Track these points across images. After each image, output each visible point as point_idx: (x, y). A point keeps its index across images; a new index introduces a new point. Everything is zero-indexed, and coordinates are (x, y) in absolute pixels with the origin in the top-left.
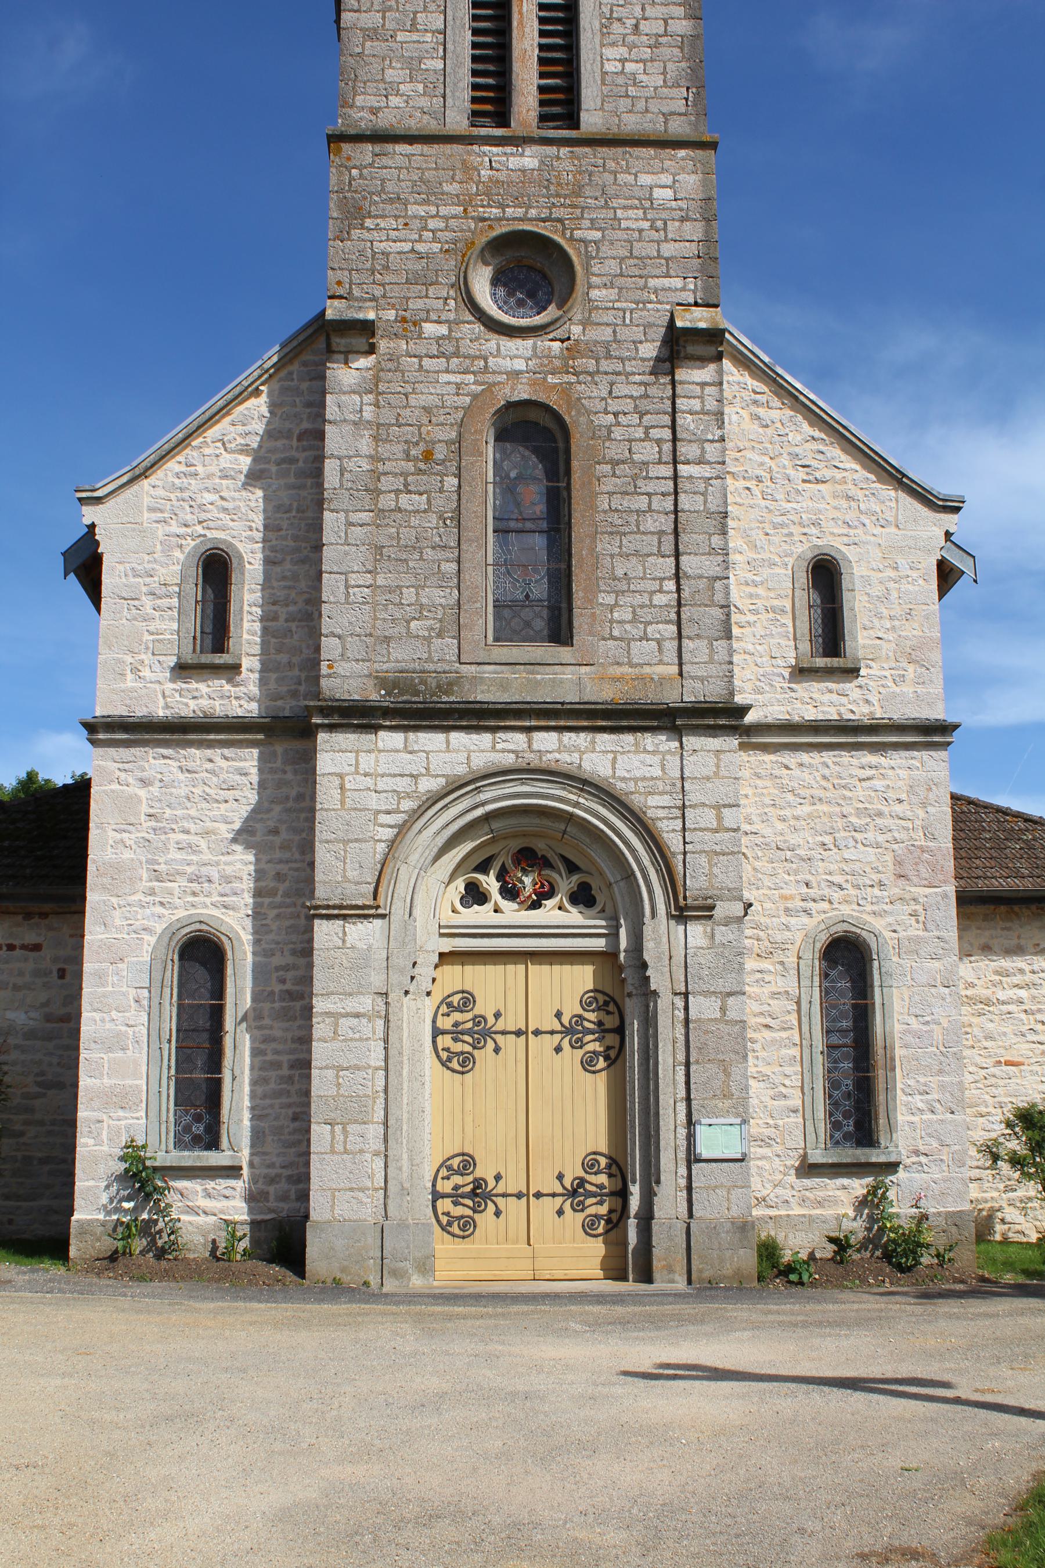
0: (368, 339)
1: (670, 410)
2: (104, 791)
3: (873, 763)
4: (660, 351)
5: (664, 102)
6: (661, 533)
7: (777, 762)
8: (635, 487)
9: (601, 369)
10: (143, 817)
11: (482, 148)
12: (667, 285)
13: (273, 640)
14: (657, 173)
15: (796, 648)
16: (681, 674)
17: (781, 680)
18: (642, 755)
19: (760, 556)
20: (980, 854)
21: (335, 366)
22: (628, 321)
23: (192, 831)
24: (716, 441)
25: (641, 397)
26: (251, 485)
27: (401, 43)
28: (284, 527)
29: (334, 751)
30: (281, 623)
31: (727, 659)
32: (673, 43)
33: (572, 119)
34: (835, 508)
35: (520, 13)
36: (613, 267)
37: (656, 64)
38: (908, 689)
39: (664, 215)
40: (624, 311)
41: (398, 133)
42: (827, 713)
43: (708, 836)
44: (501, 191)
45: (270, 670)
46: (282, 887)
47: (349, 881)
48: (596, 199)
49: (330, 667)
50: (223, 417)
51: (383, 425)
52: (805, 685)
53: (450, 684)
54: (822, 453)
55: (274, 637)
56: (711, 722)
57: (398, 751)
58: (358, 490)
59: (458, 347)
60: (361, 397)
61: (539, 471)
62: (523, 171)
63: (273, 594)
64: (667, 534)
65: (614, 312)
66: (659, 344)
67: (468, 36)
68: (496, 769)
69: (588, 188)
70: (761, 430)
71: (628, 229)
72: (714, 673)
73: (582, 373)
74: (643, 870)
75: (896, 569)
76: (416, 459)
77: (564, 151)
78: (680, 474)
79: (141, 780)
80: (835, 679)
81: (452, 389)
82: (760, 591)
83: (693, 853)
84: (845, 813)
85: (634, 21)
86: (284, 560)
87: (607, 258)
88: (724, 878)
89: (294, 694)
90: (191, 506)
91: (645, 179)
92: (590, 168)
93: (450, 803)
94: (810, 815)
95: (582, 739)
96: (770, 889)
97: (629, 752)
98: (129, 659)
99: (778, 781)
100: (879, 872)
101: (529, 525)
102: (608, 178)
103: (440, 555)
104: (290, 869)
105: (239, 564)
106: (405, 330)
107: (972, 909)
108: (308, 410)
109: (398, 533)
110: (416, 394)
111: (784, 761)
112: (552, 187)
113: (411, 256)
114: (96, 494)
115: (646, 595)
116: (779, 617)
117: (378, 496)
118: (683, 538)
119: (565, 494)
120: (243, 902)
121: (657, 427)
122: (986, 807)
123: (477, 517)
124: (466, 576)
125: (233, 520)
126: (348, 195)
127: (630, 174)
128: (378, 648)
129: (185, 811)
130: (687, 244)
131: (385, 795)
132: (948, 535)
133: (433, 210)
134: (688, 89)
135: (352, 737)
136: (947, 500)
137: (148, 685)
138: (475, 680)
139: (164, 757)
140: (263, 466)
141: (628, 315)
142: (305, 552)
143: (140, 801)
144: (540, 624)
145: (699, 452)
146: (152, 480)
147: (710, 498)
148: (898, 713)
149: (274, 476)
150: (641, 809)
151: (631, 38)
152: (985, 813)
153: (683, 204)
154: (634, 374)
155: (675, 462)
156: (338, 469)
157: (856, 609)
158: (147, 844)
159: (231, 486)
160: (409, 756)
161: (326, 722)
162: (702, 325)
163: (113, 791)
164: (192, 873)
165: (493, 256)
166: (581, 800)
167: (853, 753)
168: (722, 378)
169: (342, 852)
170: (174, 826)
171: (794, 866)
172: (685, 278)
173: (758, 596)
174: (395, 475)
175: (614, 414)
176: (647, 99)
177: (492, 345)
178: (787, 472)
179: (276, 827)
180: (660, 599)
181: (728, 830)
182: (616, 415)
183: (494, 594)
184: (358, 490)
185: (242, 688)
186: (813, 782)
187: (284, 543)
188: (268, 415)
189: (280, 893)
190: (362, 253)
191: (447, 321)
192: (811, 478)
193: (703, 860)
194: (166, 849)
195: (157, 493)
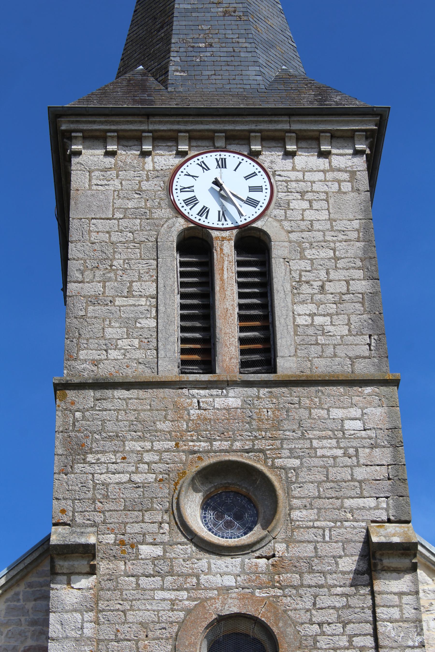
1: (371, 619)
4: (358, 565)
5: (350, 347)
11: (191, 391)
21: (58, 586)
22: (327, 538)
24: (417, 647)
25: (343, 607)
32: (355, 300)
35: (222, 280)
39: (355, 443)
40: (324, 529)
41: (117, 381)
44: (209, 427)
48: (294, 431)
51: (102, 640)
59: (172, 566)
60: (82, 615)
62: (228, 409)
65: (314, 530)
66: (357, 558)
67: (177, 299)
69: (286, 422)
71: (323, 456)
73: (287, 587)
77: (263, 391)
81: (166, 605)
85: (320, 283)
87: (305, 482)
91: (337, 413)
92: (287, 405)
102: (304, 413)
106: (123, 552)
108: (33, 629)
110: (133, 610)
112: (254, 423)
113: (128, 485)
121: (360, 635)
126: (73, 434)
127: (323, 409)
130: (378, 468)
134: (370, 336)
141: (327, 533)
153: (372, 433)
154: (335, 586)
162: (396, 540)
165: (202, 484)
168: (418, 588)
172: (377, 498)
175: (319, 624)
176: (335, 346)
177: (204, 561)
182: (320, 625)
190: (84, 485)
191: (162, 543)
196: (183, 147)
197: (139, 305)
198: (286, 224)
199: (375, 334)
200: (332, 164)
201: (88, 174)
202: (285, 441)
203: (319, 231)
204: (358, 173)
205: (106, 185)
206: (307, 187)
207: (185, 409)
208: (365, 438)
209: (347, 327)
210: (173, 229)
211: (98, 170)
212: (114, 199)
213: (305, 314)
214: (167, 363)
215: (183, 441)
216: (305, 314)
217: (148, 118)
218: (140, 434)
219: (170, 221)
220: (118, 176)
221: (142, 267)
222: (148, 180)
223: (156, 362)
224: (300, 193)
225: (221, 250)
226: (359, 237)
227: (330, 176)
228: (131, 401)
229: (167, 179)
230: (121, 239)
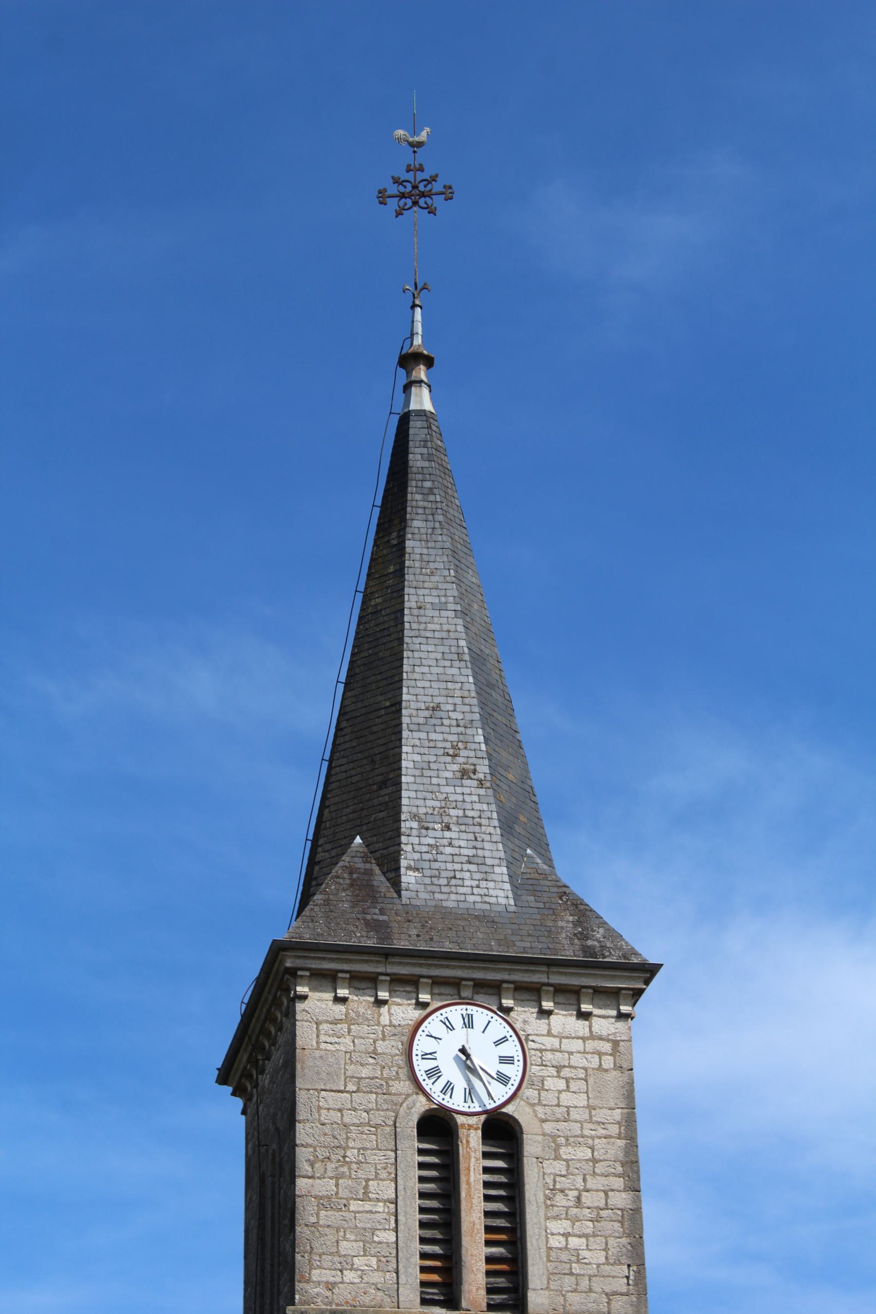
32: (614, 1217)
35: (468, 1183)
85: (576, 1193)
134: (629, 1266)
196: (424, 997)
197: (376, 1212)
198: (539, 1109)
199: (634, 1264)
200: (593, 1029)
201: (315, 1026)
204: (622, 1043)
205: (336, 1043)
206: (563, 1059)
209: (604, 1253)
210: (413, 1110)
211: (327, 1022)
212: (345, 1064)
213: (559, 1234)
214: (408, 1292)
216: (559, 1234)
217: (386, 958)
219: (410, 1099)
220: (349, 1031)
221: (378, 1158)
222: (383, 1039)
223: (396, 1288)
224: (556, 1067)
225: (468, 1142)
226: (620, 1132)
227: (591, 1045)
229: (405, 1039)
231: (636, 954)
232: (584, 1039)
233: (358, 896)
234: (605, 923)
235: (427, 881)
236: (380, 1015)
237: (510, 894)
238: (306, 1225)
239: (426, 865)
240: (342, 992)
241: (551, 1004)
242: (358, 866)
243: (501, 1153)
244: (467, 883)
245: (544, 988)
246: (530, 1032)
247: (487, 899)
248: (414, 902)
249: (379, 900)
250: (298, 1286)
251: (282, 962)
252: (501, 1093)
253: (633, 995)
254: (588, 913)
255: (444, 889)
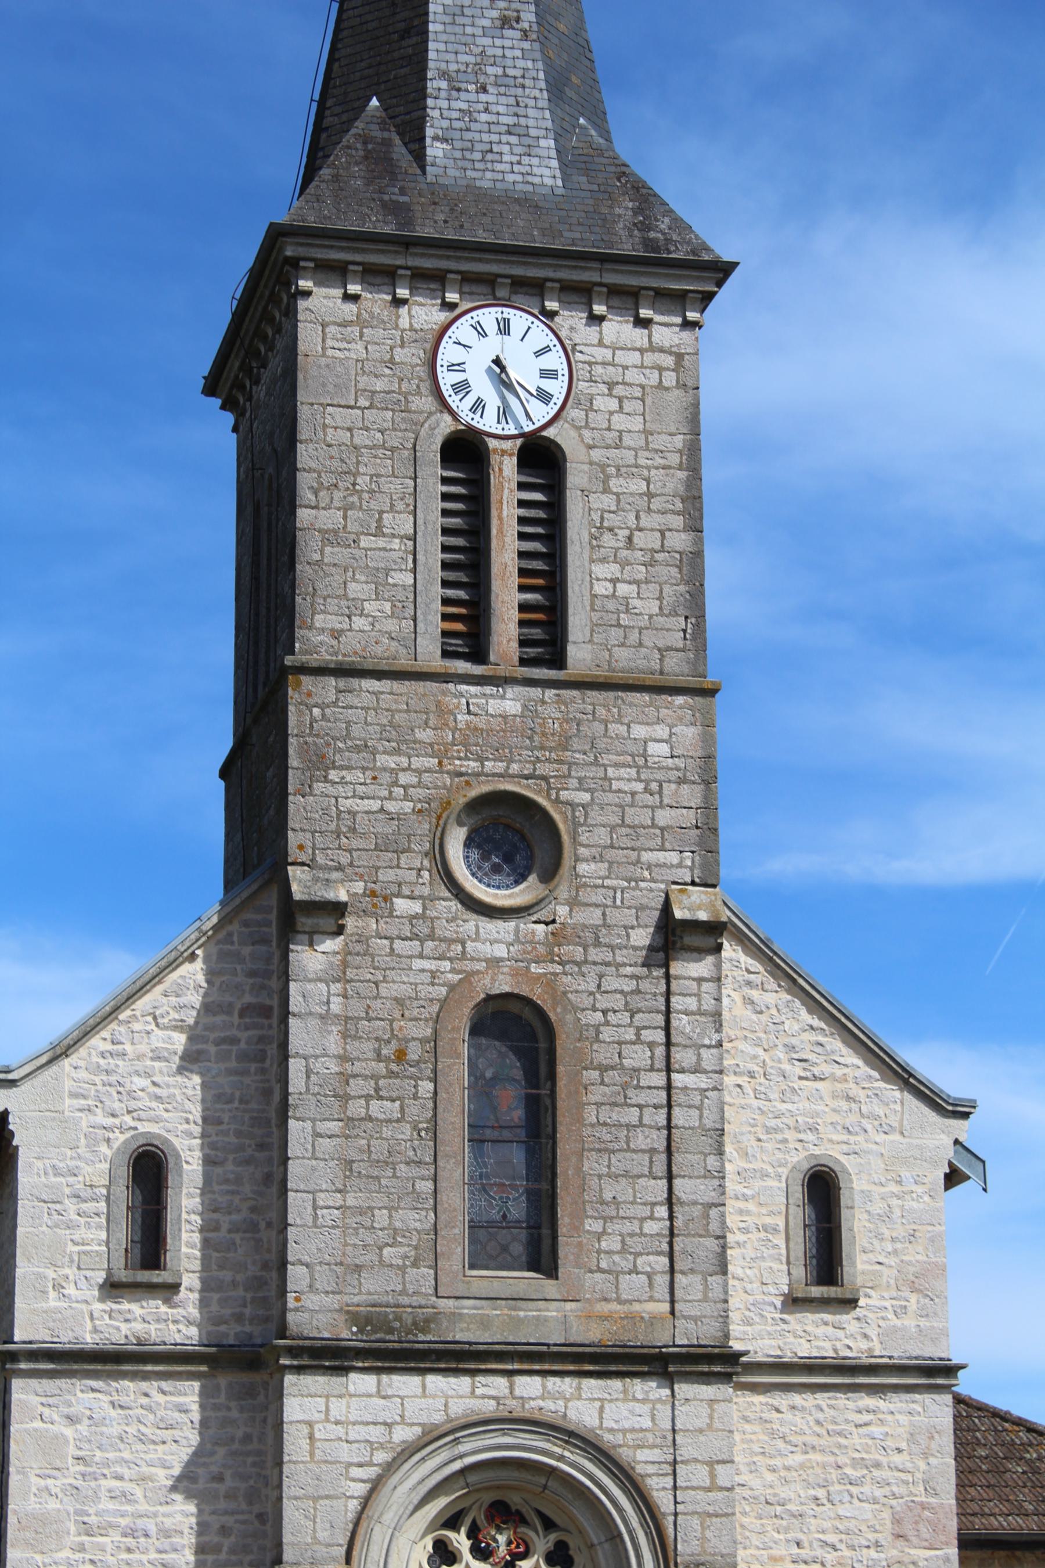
0: (337, 920)
1: (663, 1008)
2: (25, 1430)
3: (872, 1407)
4: (653, 939)
6: (652, 1151)
7: (767, 1404)
8: (625, 1097)
9: (590, 959)
10: (70, 1460)
11: (459, 687)
12: (662, 860)
13: (215, 1254)
14: (653, 724)
15: (789, 1274)
16: (672, 1312)
17: (772, 1309)
18: (631, 1404)
19: (751, 1166)
20: (975, 1480)
21: (299, 948)
22: (618, 902)
23: (126, 1477)
25: (632, 992)
26: (187, 1070)
27: (366, 550)
28: (226, 1120)
29: (302, 1396)
30: (223, 1233)
31: (722, 1297)
33: (557, 658)
34: (834, 1110)
35: (500, 518)
36: (602, 836)
37: (651, 586)
38: (909, 1322)
39: (659, 776)
41: (366, 667)
42: (823, 1348)
43: (700, 1495)
44: (480, 741)
45: (212, 1290)
46: (227, 1543)
47: (320, 1543)
48: (585, 754)
49: (297, 1299)
50: (154, 986)
51: (351, 1018)
52: (799, 1316)
53: (427, 1321)
54: (821, 1045)
55: (218, 1251)
56: (705, 1368)
57: (370, 1396)
58: (326, 1096)
59: (433, 928)
60: (328, 986)
61: (518, 1074)
62: (504, 717)
63: (214, 1200)
64: (659, 1152)
65: (604, 891)
66: (652, 930)
68: (475, 1418)
69: (575, 740)
70: (754, 1017)
71: (620, 791)
72: (709, 1312)
73: (569, 962)
74: (630, 1532)
75: (900, 1183)
76: (387, 1060)
77: (550, 693)
78: (674, 1084)
79: (68, 1417)
80: (831, 1309)
81: (426, 977)
82: (751, 1206)
83: (685, 1514)
84: (840, 1463)
85: (627, 532)
86: (226, 1160)
87: (596, 825)
88: (718, 1544)
89: (239, 1318)
90: (119, 1093)
91: (639, 731)
92: (579, 716)
93: (427, 1456)
94: (802, 1466)
95: (566, 1385)
96: (758, 1548)
97: (617, 1400)
98: (51, 1274)
99: (768, 1426)
100: (876, 1531)
101: (506, 1134)
102: (598, 727)
103: (415, 1171)
104: (236, 1521)
105: (176, 1164)
107: (969, 1553)
108: (251, 981)
109: (369, 1146)
110: (387, 982)
111: (776, 1403)
112: (536, 738)
113: (380, 816)
114: (10, 1076)
115: (636, 1223)
116: (770, 1237)
117: (347, 1102)
118: (677, 1158)
119: (548, 1102)
120: (183, 1560)
121: (650, 1027)
122: (979, 1409)
123: (455, 1129)
124: (442, 1197)
125: (167, 1110)
126: (310, 740)
127: (622, 724)
128: (348, 1278)
129: (118, 1454)
130: (684, 811)
131: (356, 1445)
132: (957, 1142)
133: (404, 761)
134: (686, 618)
135: (321, 1379)
136: (957, 1105)
137: (74, 1305)
138: (455, 1317)
139: (93, 1390)
140: (200, 1047)
141: (619, 895)
142: (249, 1151)
143: (67, 1441)
144: (518, 1249)
145: (694, 1058)
146: (73, 1059)
147: (706, 1113)
148: (899, 1351)
149: (213, 1059)
150: (629, 1464)
151: (623, 553)
152: (979, 1417)
153: (680, 763)
154: (624, 965)
155: (669, 1070)
156: (304, 1070)
157: (856, 1229)
158: (75, 1492)
159: (165, 1070)
160: (382, 1402)
161: (295, 1363)
162: (703, 916)
163: (36, 1430)
164: (127, 1526)
165: (468, 816)
166: (567, 1454)
167: (850, 1395)
168: (721, 973)
169: (312, 1511)
170: (105, 1471)
171: (784, 1523)
172: (681, 852)
173: (748, 1213)
174: (366, 1078)
175: (603, 1012)
177: (470, 926)
178: (783, 1066)
179: (221, 1473)
180: (651, 1227)
181: (722, 1489)
182: (605, 1012)
183: (469, 1213)
184: (326, 1096)
185: (180, 1310)
186: (805, 1427)
187: (226, 1139)
188: (205, 985)
189: (225, 1549)
190: (325, 811)
191: (421, 897)
192: (808, 1074)
193: (696, 1522)
194: (96, 1497)
195: (79, 1076)
196: (452, 297)
197: (391, 550)
198: (586, 433)
199: (692, 616)
201: (320, 328)
202: (574, 767)
203: (629, 448)
204: (687, 357)
206: (617, 374)
207: (451, 712)
208: (672, 769)
209: (658, 602)
210: (436, 431)
211: (335, 323)
212: (356, 374)
213: (606, 579)
214: (427, 642)
215: (448, 758)
217: (407, 248)
218: (394, 744)
219: (433, 418)
220: (361, 336)
222: (402, 346)
224: (608, 384)
225: (500, 470)
226: (681, 462)
227: (650, 358)
228: (382, 696)
229: (428, 346)
230: (368, 442)
231: (707, 249)
232: (641, 351)
233: (373, 171)
234: (672, 211)
235: (458, 154)
236: (398, 317)
237: (558, 174)
238: (309, 563)
239: (457, 135)
240: (353, 288)
241: (604, 308)
242: (373, 134)
243: (540, 485)
244: (506, 158)
245: (596, 289)
246: (577, 341)
247: (530, 179)
248: (441, 180)
249: (399, 177)
250: (299, 633)
251: (281, 249)
252: (541, 413)
253: (702, 300)
254: (652, 199)
255: (478, 165)
